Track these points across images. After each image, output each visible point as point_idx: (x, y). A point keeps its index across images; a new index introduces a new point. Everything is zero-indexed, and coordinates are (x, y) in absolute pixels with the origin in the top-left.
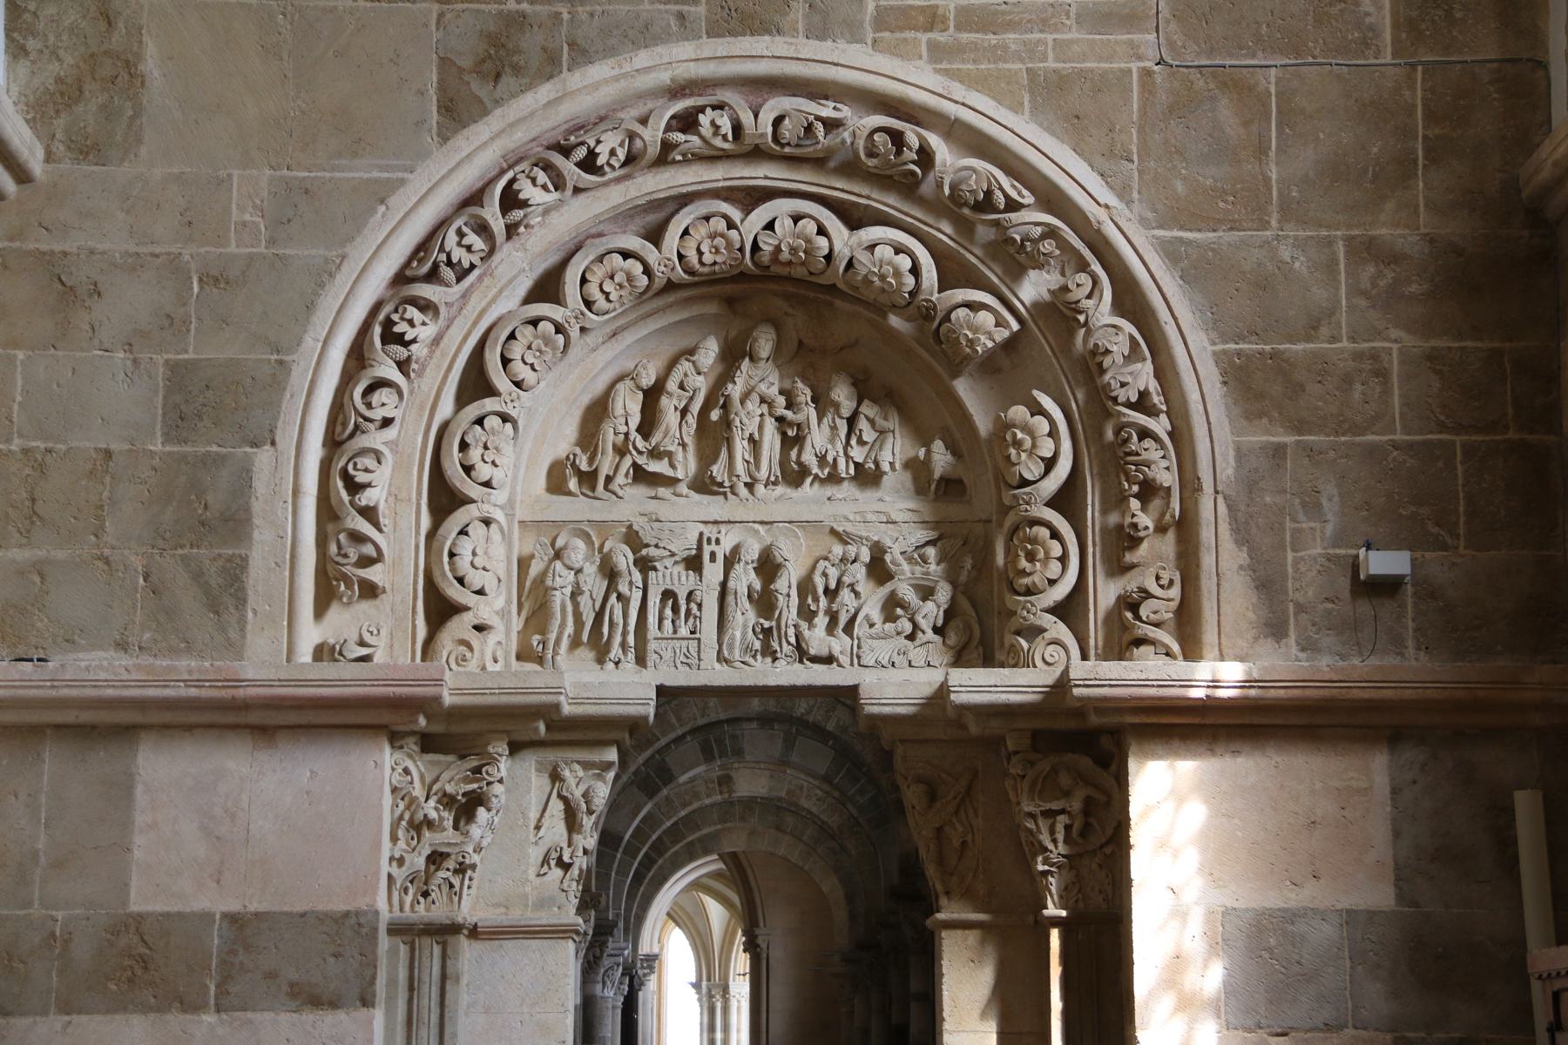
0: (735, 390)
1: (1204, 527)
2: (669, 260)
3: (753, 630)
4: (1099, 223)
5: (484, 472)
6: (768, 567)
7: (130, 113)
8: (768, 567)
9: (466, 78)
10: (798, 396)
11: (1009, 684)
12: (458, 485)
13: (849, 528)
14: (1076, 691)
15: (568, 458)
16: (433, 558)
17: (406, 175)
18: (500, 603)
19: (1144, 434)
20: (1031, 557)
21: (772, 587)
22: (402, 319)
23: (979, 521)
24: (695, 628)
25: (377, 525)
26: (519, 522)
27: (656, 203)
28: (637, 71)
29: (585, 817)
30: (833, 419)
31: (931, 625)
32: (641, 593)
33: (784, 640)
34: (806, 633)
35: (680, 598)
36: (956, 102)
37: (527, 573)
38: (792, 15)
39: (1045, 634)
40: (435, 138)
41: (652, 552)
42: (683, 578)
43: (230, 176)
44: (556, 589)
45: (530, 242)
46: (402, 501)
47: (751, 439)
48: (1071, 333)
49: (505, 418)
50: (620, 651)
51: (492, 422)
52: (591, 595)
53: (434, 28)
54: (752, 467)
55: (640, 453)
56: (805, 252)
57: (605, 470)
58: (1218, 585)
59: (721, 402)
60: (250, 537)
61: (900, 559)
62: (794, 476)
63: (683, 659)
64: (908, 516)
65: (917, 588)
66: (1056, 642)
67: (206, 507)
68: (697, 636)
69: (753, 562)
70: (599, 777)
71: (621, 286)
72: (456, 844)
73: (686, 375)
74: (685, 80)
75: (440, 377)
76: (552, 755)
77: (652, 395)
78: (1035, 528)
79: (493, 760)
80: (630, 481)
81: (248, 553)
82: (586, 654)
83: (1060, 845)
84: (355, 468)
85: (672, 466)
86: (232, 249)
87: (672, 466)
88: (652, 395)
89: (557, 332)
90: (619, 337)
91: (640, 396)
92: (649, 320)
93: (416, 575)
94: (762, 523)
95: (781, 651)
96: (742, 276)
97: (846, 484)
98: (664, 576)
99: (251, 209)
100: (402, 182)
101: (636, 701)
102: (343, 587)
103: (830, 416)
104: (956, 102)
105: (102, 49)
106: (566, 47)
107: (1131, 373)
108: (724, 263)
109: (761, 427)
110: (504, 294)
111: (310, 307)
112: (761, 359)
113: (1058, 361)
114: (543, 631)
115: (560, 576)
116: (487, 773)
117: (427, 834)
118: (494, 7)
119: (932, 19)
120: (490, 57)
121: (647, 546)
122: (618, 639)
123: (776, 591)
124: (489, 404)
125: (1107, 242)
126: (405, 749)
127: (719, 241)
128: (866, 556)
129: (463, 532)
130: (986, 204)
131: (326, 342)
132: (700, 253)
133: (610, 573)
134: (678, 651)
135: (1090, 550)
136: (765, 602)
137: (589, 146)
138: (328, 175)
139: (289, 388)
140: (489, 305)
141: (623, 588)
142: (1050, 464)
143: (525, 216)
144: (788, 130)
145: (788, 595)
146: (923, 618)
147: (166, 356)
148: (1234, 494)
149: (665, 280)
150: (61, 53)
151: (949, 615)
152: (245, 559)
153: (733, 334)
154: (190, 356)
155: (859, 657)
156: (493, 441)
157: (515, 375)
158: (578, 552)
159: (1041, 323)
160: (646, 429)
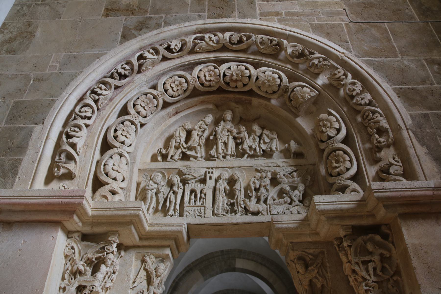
0: (219, 129)
1: (407, 140)
2: (194, 78)
3: (227, 204)
4: (342, 57)
5: (122, 138)
6: (232, 182)
7: (28, 43)
8: (232, 182)
9: (131, 30)
10: (241, 129)
11: (341, 200)
12: (111, 142)
13: (262, 168)
14: (376, 195)
15: (158, 150)
16: (98, 167)
17: (107, 52)
19: (374, 112)
20: (337, 161)
21: (234, 187)
22: (98, 87)
23: (311, 165)
24: (203, 202)
25: (76, 150)
26: (139, 169)
27: (191, 66)
28: (185, 27)
29: (155, 278)
32: (182, 191)
34: (248, 203)
35: (197, 192)
36: (288, 31)
37: (140, 186)
38: (234, 14)
39: (349, 187)
40: (119, 43)
41: (187, 176)
42: (199, 185)
43: (52, 55)
44: (149, 190)
45: (147, 74)
46: (89, 147)
48: (339, 90)
49: (132, 123)
50: (173, 212)
52: (163, 194)
53: (123, 21)
54: (225, 151)
55: (185, 148)
56: (241, 76)
57: (171, 153)
58: (419, 160)
59: (214, 134)
60: (25, 153)
61: (283, 177)
62: (240, 154)
63: (198, 214)
65: (290, 186)
66: (354, 190)
67: (12, 144)
68: (204, 205)
69: (226, 180)
70: (162, 261)
71: (177, 86)
72: (90, 281)
73: (201, 124)
74: (200, 28)
76: (142, 252)
78: (337, 152)
79: (110, 243)
80: (180, 157)
81: (23, 158)
82: (160, 215)
83: (372, 276)
84: (71, 130)
85: (196, 152)
86: (47, 72)
87: (196, 152)
89: (154, 98)
90: (179, 114)
91: (185, 133)
92: (189, 110)
93: (90, 172)
94: (229, 168)
95: (238, 210)
96: (220, 90)
98: (191, 185)
99: (56, 62)
100: (106, 53)
101: (177, 225)
102: (56, 169)
103: (253, 136)
104: (288, 31)
105: (26, 31)
106: (163, 23)
107: (364, 95)
108: (214, 81)
109: (228, 139)
110: (137, 88)
111: (67, 85)
112: (228, 120)
113: (335, 101)
115: (151, 186)
116: (107, 249)
117: (78, 276)
118: (142, 16)
119: (277, 14)
120: (139, 26)
121: (185, 175)
122: (172, 208)
123: (236, 189)
124: (126, 117)
125: (346, 62)
126: (73, 238)
127: (211, 72)
128: (269, 175)
129: (111, 157)
130: (301, 55)
131: (70, 95)
132: (205, 76)
133: (171, 185)
134: (196, 211)
135: (361, 157)
136: (231, 194)
137: (168, 44)
138: (82, 53)
139: (54, 106)
140: (131, 90)
141: (175, 188)
142: (338, 131)
143: (145, 62)
144: (234, 38)
145: (240, 190)
147: (15, 100)
148: (414, 129)
149: (193, 85)
150: (13, 32)
151: (304, 195)
152: (21, 160)
153: (218, 116)
154: (23, 99)
155: (270, 211)
156: (126, 129)
157: (137, 109)
158: (159, 177)
159: (326, 90)
160: (186, 142)
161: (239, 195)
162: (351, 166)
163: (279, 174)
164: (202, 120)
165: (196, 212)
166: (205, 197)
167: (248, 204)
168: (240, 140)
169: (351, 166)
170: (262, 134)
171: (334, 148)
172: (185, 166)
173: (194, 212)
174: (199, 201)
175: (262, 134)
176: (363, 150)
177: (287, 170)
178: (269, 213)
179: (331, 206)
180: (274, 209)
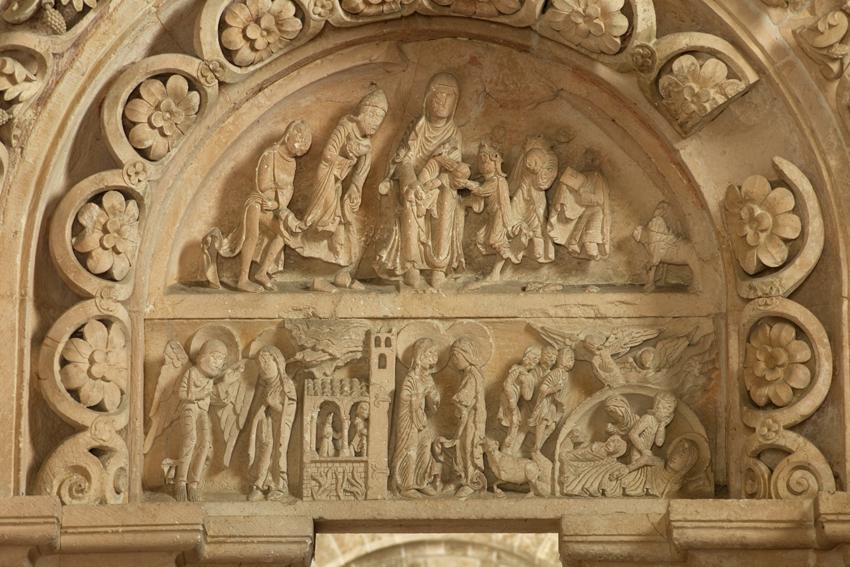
0: (411, 156)
5: (103, 261)
6: (450, 375)
8: (450, 375)
12: (71, 276)
13: (549, 324)
18: (122, 421)
21: (455, 397)
30: (529, 191)
31: (650, 444)
32: (295, 406)
33: (469, 463)
41: (308, 356)
47: (428, 215)
49: (128, 194)
50: (270, 478)
51: (113, 200)
55: (293, 234)
57: (250, 254)
59: (392, 171)
62: (478, 261)
63: (346, 485)
64: (622, 310)
68: (364, 458)
71: (269, 32)
73: (348, 138)
75: (48, 145)
77: (307, 163)
80: (281, 268)
85: (332, 249)
88: (307, 163)
89: (192, 87)
94: (443, 319)
95: (466, 477)
97: (545, 271)
110: (126, 42)
114: (176, 455)
115: (197, 386)
121: (302, 348)
122: (267, 463)
124: (112, 178)
128: (568, 360)
129: (78, 334)
133: (259, 384)
134: (340, 477)
136: (446, 417)
140: (107, 55)
142: (795, 247)
145: (475, 408)
146: (640, 435)
149: (323, 22)
155: (561, 484)
156: (114, 223)
157: (140, 142)
160: (300, 205)
161: (471, 424)
163: (597, 352)
164: (352, 120)
165: (340, 481)
166: (365, 431)
168: (483, 204)
170: (556, 183)
172: (300, 310)
173: (334, 481)
174: (349, 444)
175: (556, 183)
178: (558, 488)
180: (572, 478)
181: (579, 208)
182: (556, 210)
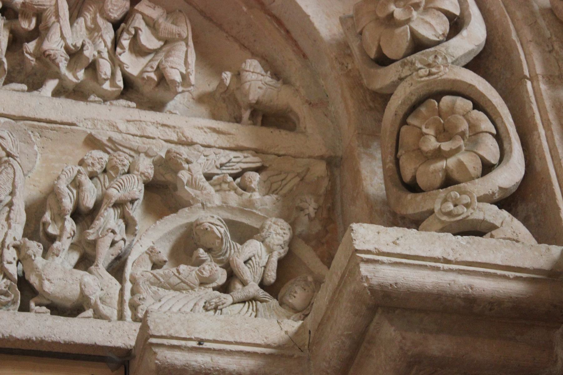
11: (470, 259)
13: (116, 137)
30: (94, 20)
31: (258, 279)
34: (39, 261)
64: (212, 138)
65: (230, 224)
78: (446, 100)
103: (89, 16)
135: (542, 131)
146: (245, 262)
155: (134, 307)
162: (501, 161)
163: (186, 166)
167: (40, 266)
168: (34, 21)
169: (501, 161)
170: (126, 18)
171: (435, 81)
176: (554, 106)
177: (224, 160)
178: (128, 313)
179: (425, 272)
181: (156, 41)
182: (129, 33)
